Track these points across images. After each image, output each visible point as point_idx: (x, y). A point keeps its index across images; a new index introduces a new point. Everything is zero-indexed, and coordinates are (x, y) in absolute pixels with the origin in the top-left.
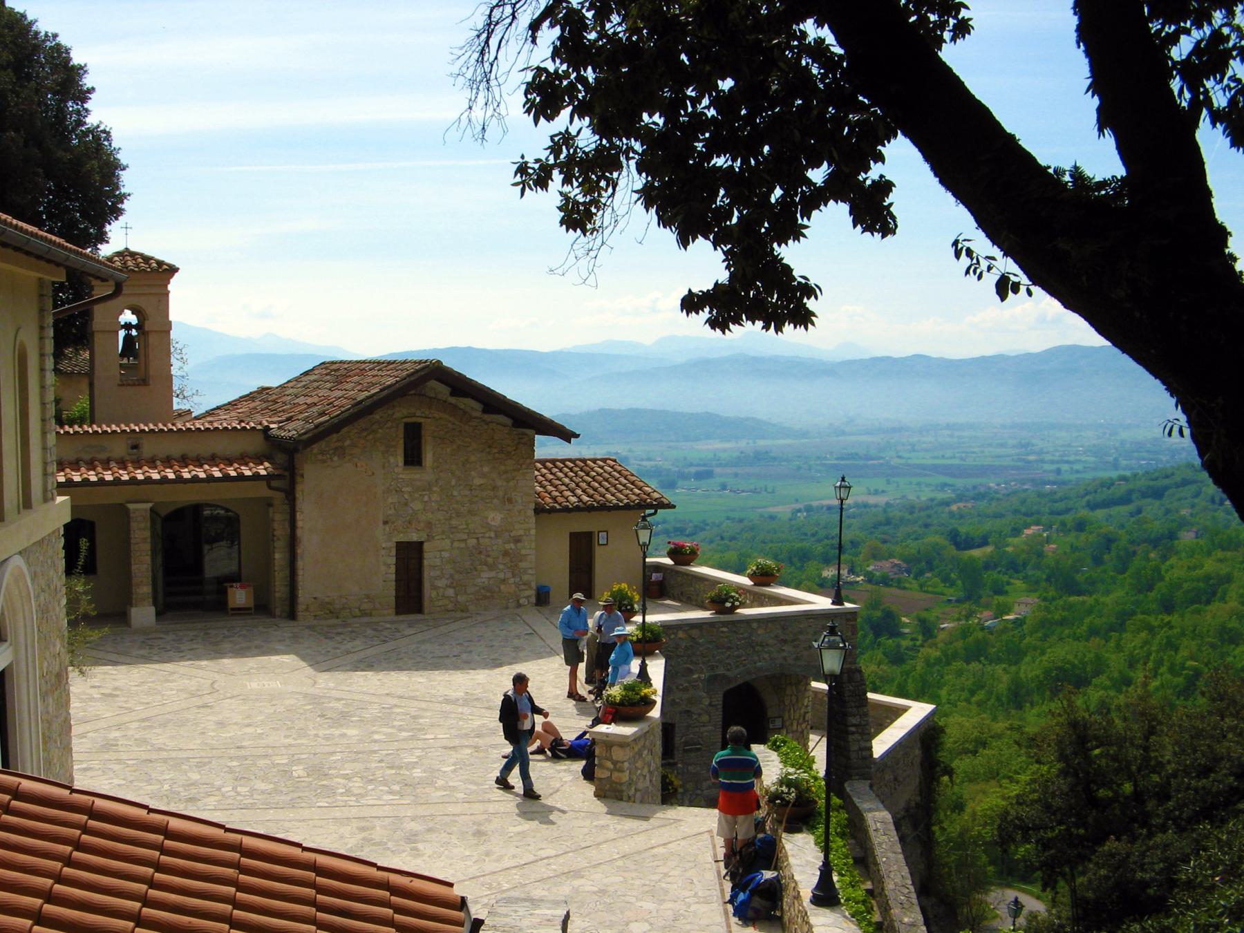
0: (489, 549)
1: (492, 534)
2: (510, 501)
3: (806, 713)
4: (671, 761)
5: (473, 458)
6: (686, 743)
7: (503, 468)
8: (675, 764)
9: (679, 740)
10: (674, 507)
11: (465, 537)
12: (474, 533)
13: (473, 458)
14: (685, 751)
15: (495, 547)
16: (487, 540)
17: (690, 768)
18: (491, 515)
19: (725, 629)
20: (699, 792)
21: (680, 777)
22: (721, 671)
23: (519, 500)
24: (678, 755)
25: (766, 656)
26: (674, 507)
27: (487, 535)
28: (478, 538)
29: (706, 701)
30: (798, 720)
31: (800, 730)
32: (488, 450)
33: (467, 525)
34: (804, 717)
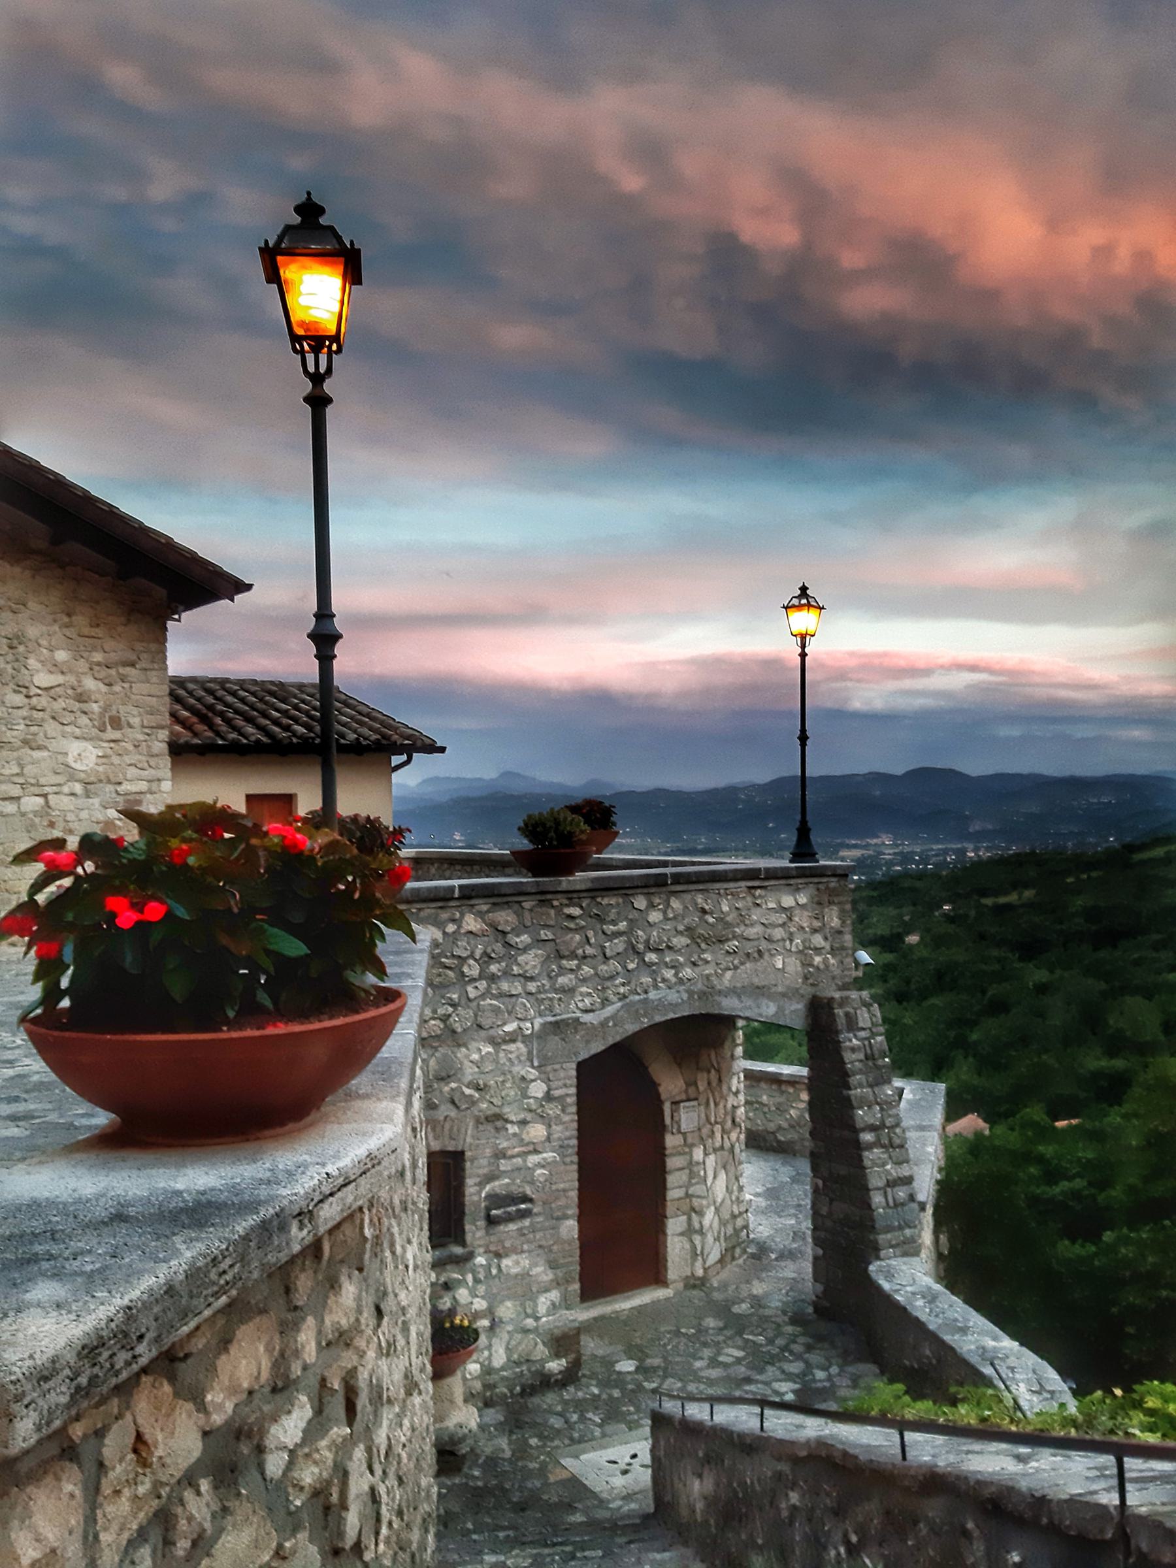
0: (70, 817)
1: (78, 788)
2: (116, 723)
3: (734, 1108)
4: (458, 1250)
5: (32, 631)
6: (496, 1200)
7: (98, 657)
8: (470, 1256)
9: (475, 1193)
10: (442, 750)
11: (16, 791)
12: (38, 785)
13: (32, 631)
14: (491, 1221)
15: (84, 815)
16: (66, 799)
17: (506, 1262)
18: (74, 748)
19: (576, 911)
20: (530, 1323)
21: (481, 1289)
22: (572, 1010)
23: (136, 721)
24: (475, 1231)
25: (669, 974)
26: (442, 750)
27: (66, 789)
28: (45, 796)
29: (538, 1089)
30: (723, 1124)
31: (727, 1144)
32: (66, 619)
33: (22, 767)
34: (733, 1121)
